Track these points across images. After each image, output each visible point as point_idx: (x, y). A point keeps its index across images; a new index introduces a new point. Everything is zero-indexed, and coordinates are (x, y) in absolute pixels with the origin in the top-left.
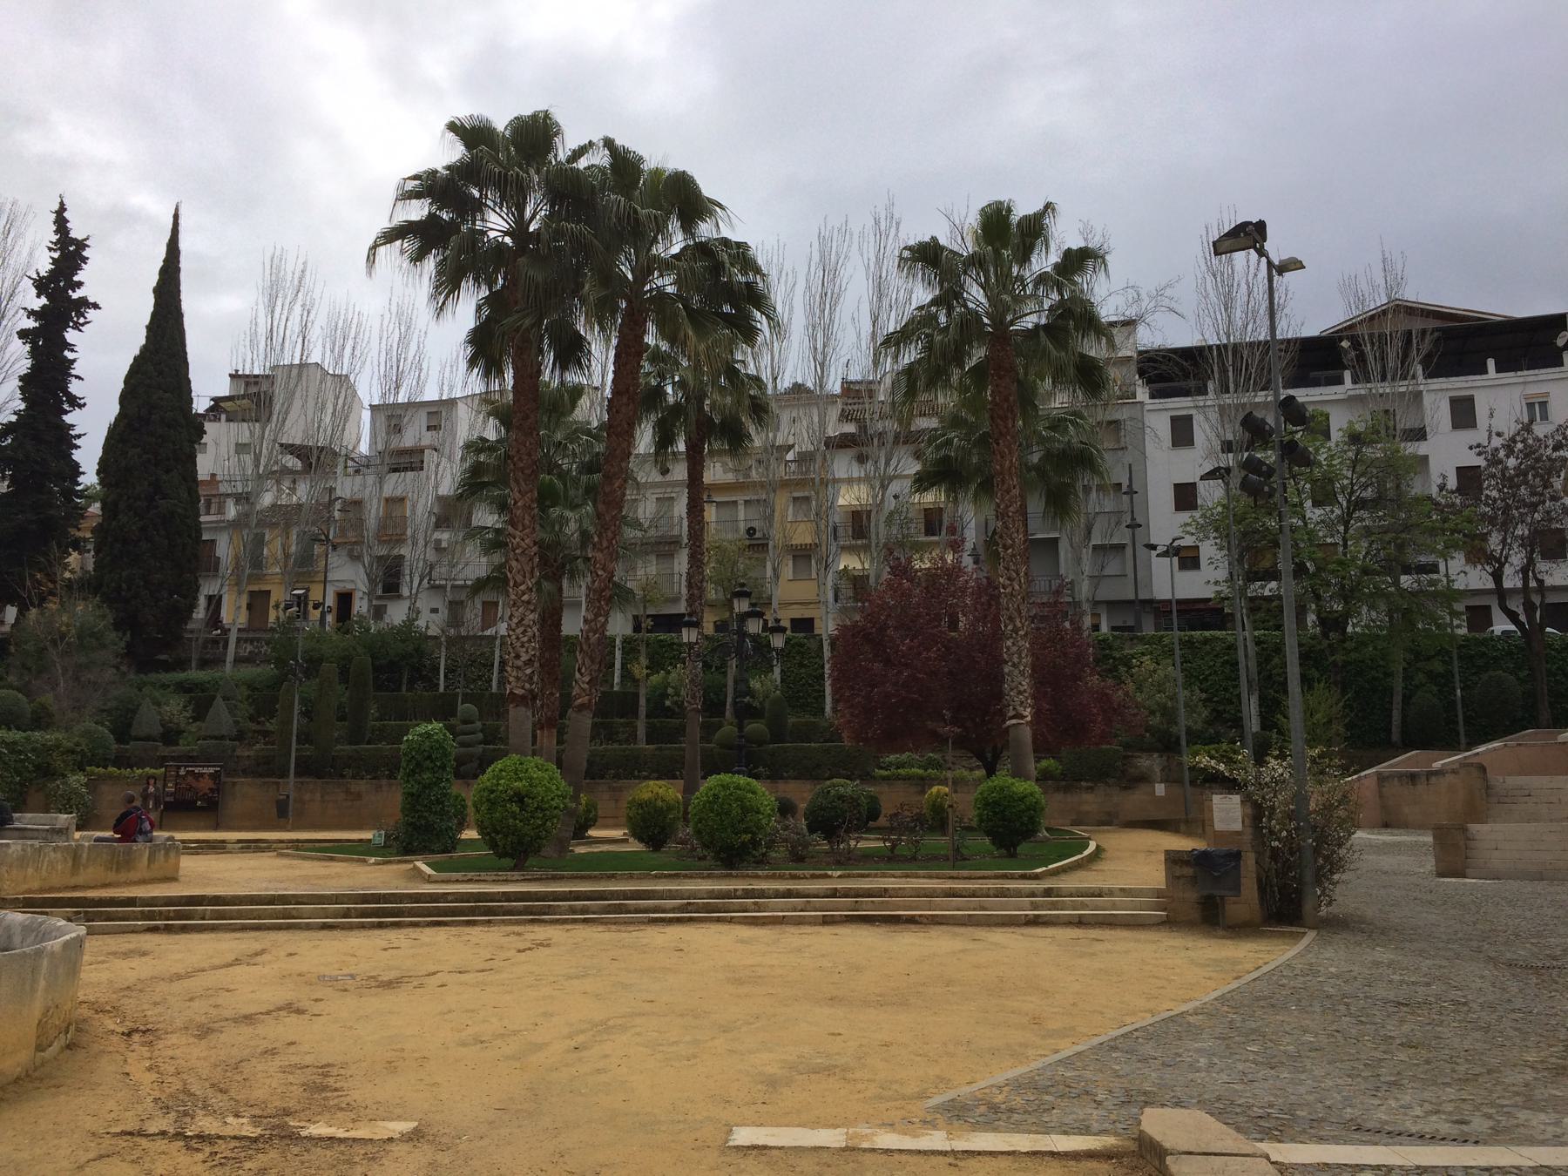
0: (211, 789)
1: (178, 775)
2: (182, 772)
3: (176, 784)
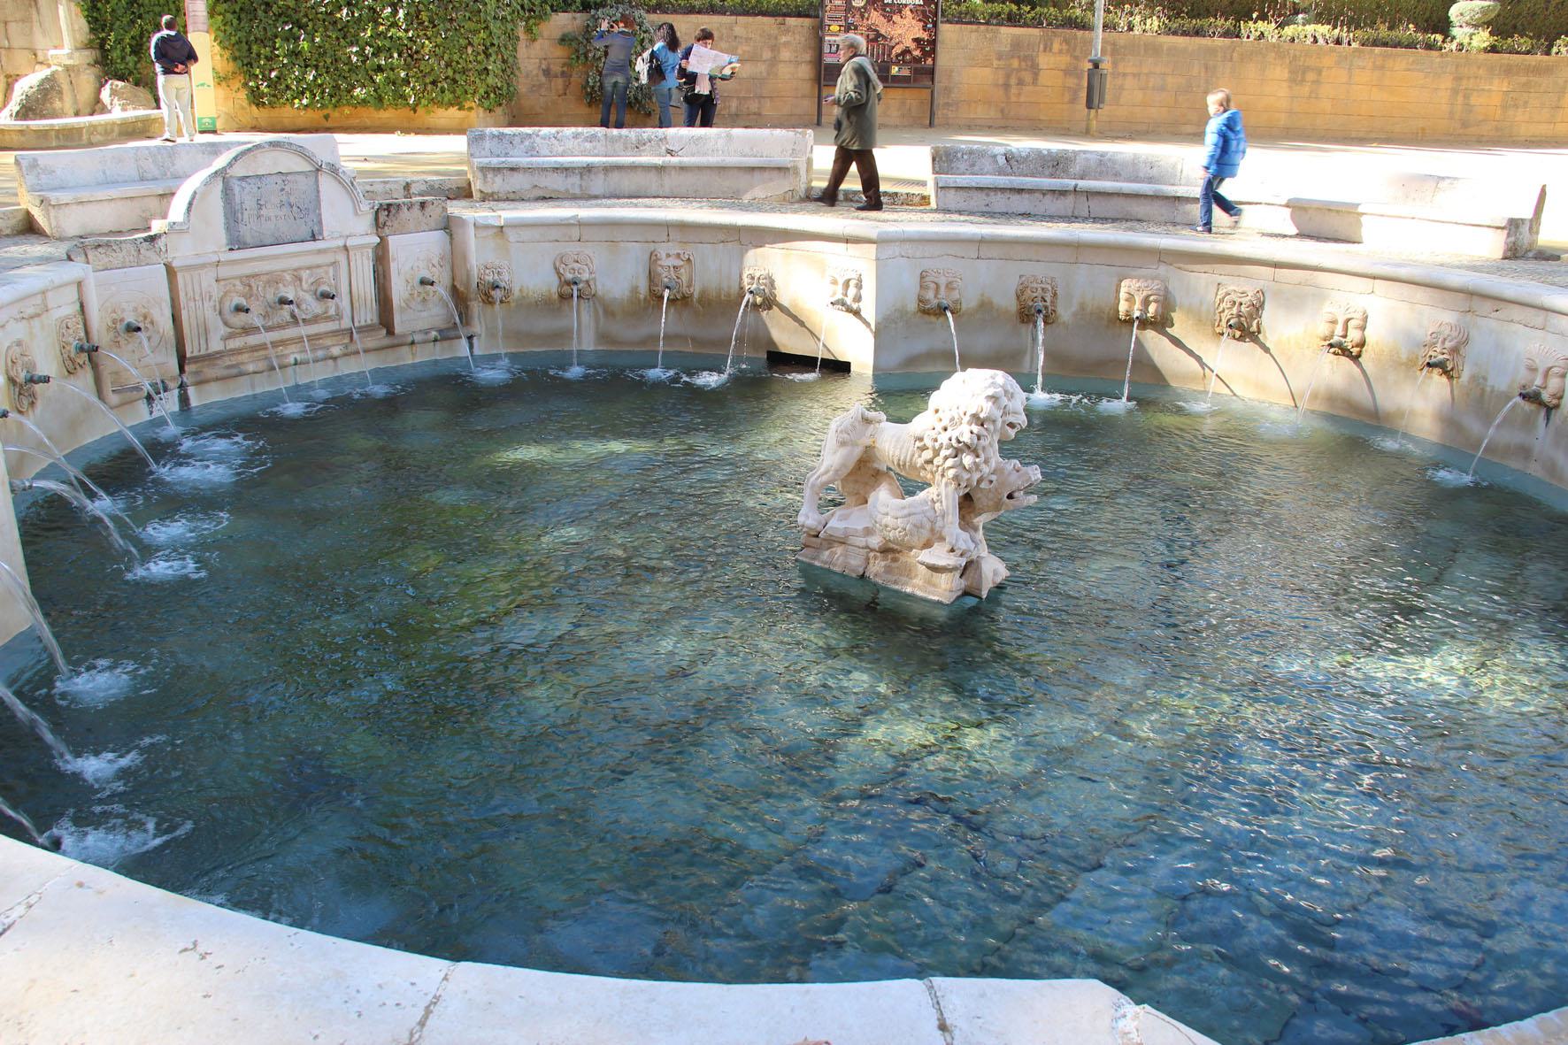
0: (917, 40)
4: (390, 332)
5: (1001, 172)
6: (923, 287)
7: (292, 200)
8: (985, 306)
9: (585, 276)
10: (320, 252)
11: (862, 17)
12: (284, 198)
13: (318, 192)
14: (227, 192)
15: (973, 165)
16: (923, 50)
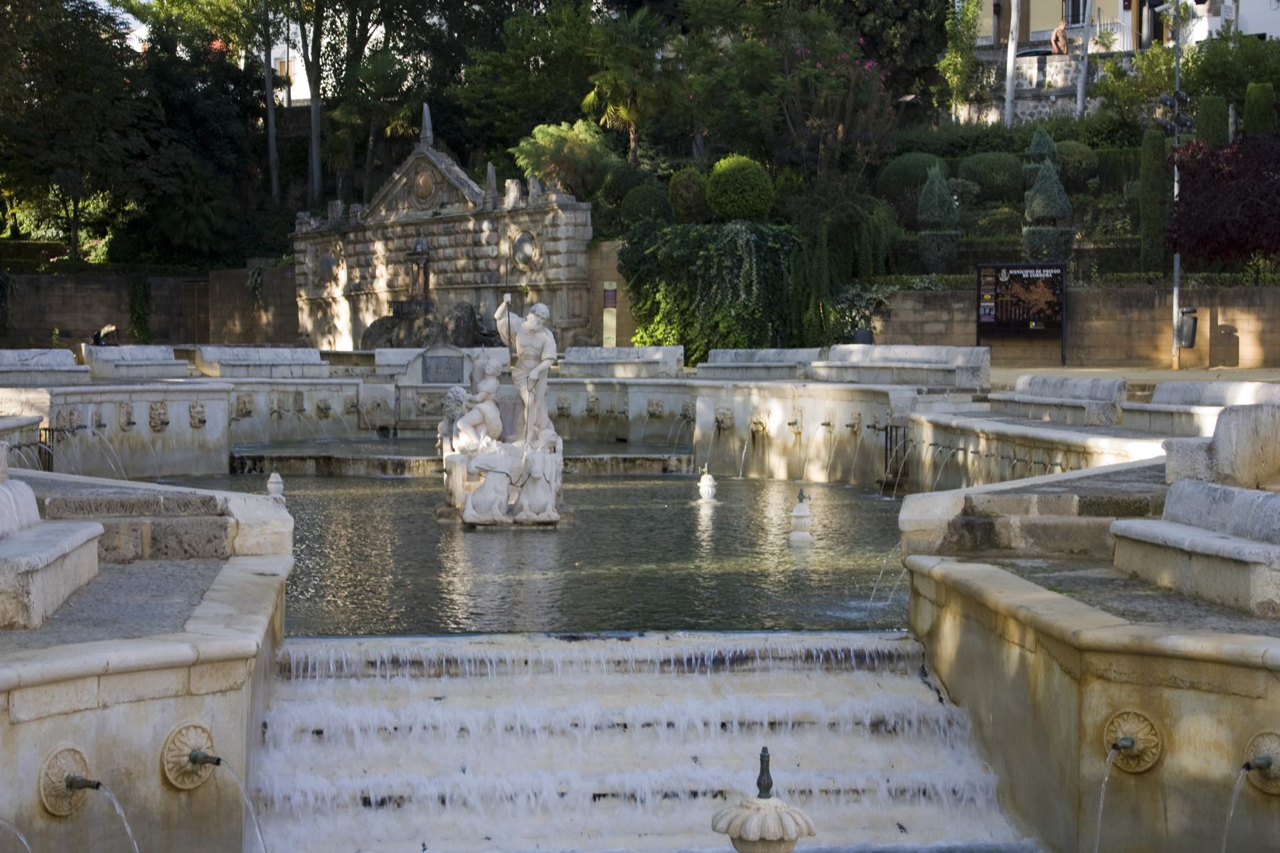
0: (1048, 303)
1: (997, 282)
2: (1004, 277)
3: (997, 296)
5: (732, 361)
8: (672, 415)
9: (566, 406)
11: (1007, 288)
14: (424, 363)
16: (1053, 309)
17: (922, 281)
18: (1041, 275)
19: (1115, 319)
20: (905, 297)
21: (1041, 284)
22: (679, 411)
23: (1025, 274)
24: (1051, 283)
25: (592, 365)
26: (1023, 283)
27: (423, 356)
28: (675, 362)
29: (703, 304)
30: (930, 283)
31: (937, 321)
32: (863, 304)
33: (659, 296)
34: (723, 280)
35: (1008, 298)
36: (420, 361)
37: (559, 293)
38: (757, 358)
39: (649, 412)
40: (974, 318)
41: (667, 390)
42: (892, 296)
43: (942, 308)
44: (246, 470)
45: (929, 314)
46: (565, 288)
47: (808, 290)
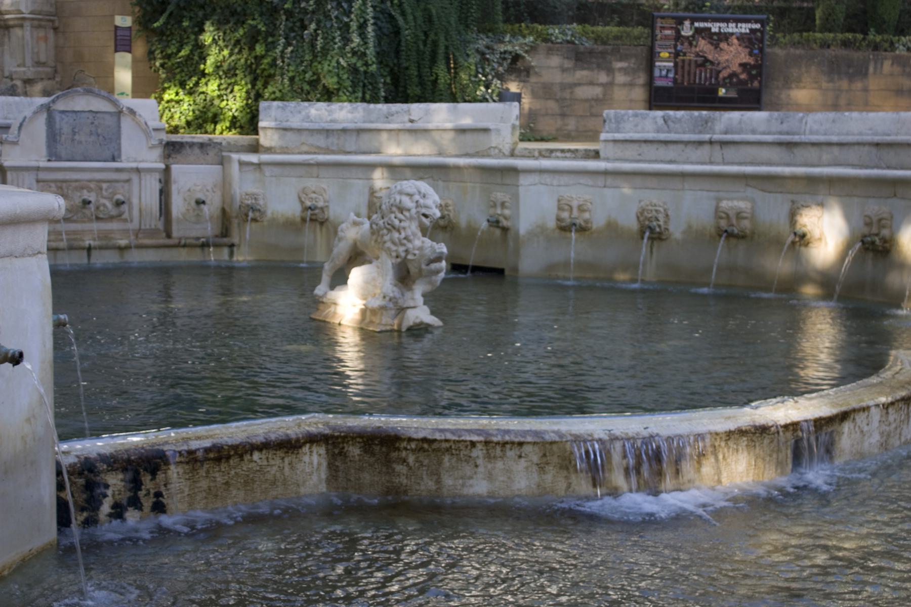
0: (743, 65)
1: (678, 37)
2: (687, 30)
3: (677, 54)
4: (169, 236)
5: (658, 131)
6: (560, 209)
7: (100, 131)
8: (612, 227)
9: (321, 204)
10: (118, 170)
11: (691, 44)
12: (93, 129)
13: (119, 127)
14: (50, 122)
15: (636, 126)
16: (749, 74)
17: (563, 33)
18: (735, 30)
19: (820, 88)
20: (550, 51)
21: (735, 41)
22: (630, 222)
23: (715, 27)
24: (747, 40)
25: (328, 132)
26: (711, 38)
27: (48, 108)
28: (510, 130)
29: (290, 49)
30: (572, 35)
31: (592, 83)
32: (495, 58)
33: (207, 38)
34: (327, 16)
35: (691, 57)
36: (43, 118)
37: (18, 32)
38: (719, 126)
39: (559, 219)
40: (642, 79)
41: (600, 181)
42: (532, 49)
43: (599, 67)
44: (106, 508)
45: (582, 74)
46: (27, 24)
47: (432, 36)
